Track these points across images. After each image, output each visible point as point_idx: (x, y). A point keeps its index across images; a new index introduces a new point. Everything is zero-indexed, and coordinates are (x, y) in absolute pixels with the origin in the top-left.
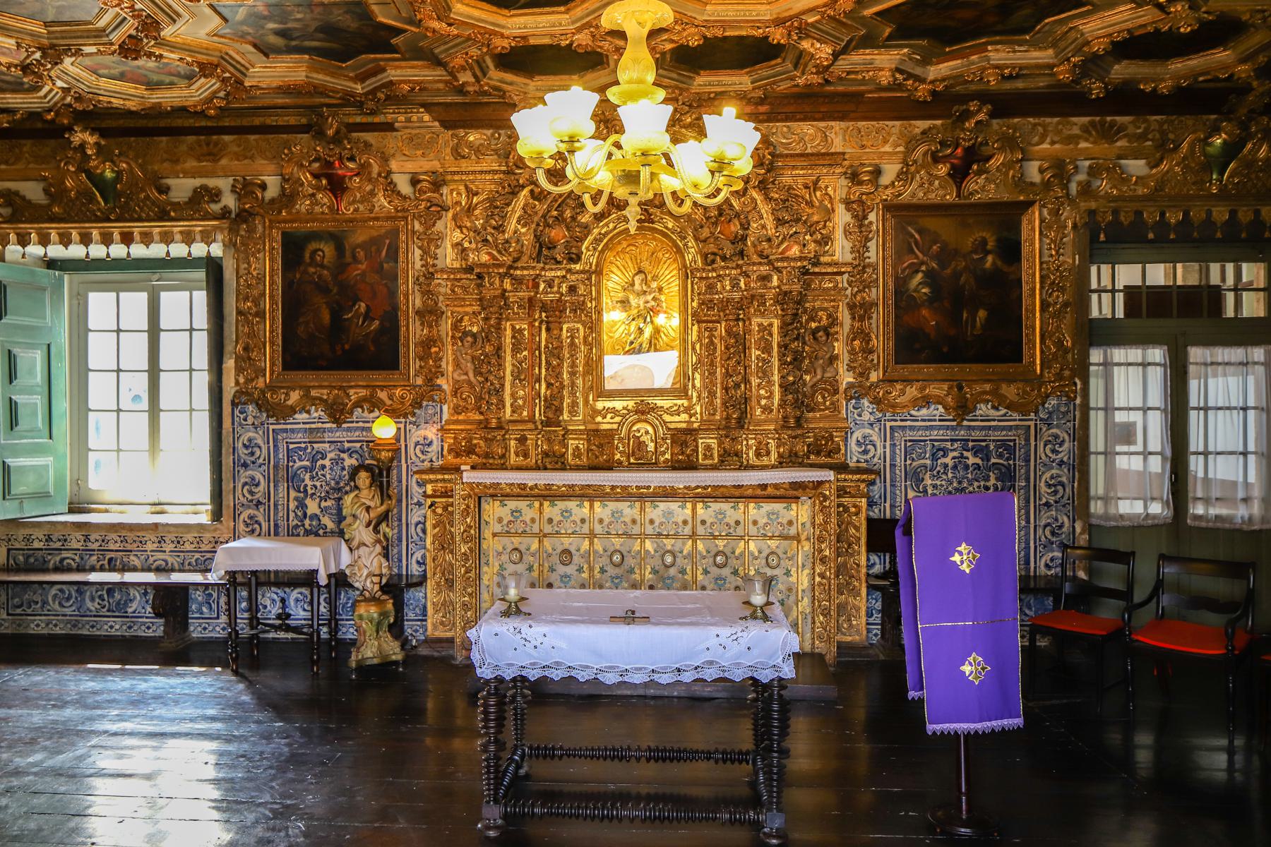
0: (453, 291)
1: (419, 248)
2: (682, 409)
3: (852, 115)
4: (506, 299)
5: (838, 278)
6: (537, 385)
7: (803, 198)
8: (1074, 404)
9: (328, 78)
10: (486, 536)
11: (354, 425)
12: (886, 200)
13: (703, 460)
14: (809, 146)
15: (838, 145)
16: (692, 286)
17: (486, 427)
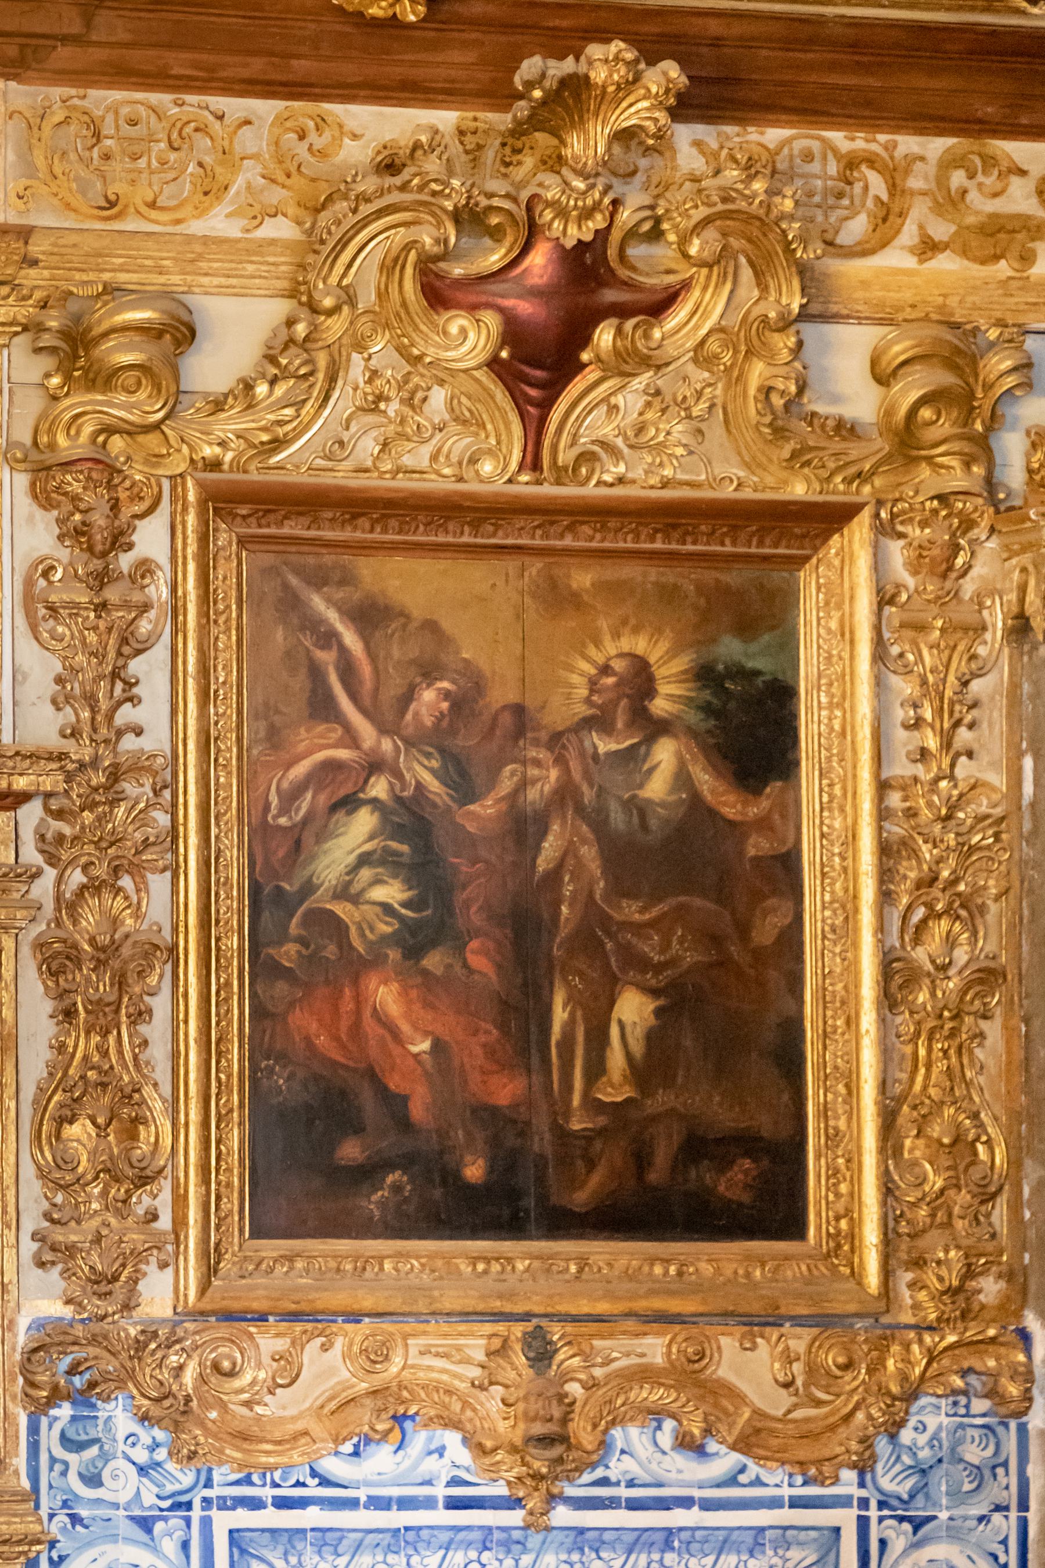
3: (63, 54)
8: (1022, 1429)
12: (215, 465)
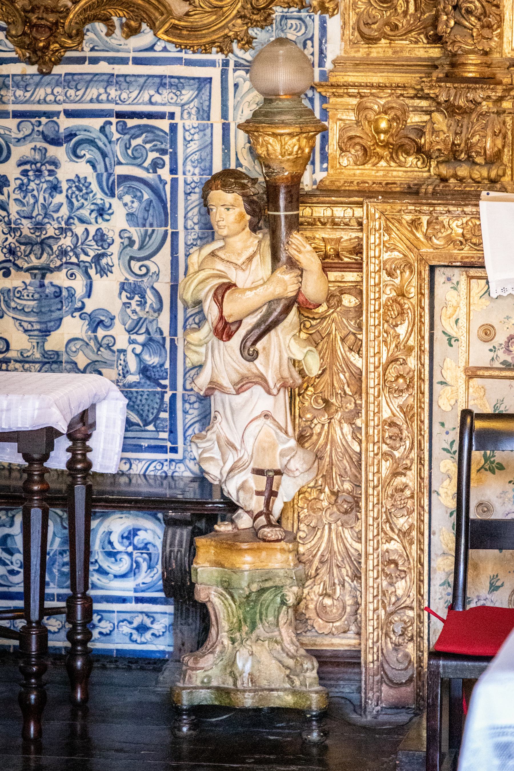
10: (448, 377)
11: (87, 68)
17: (449, 77)
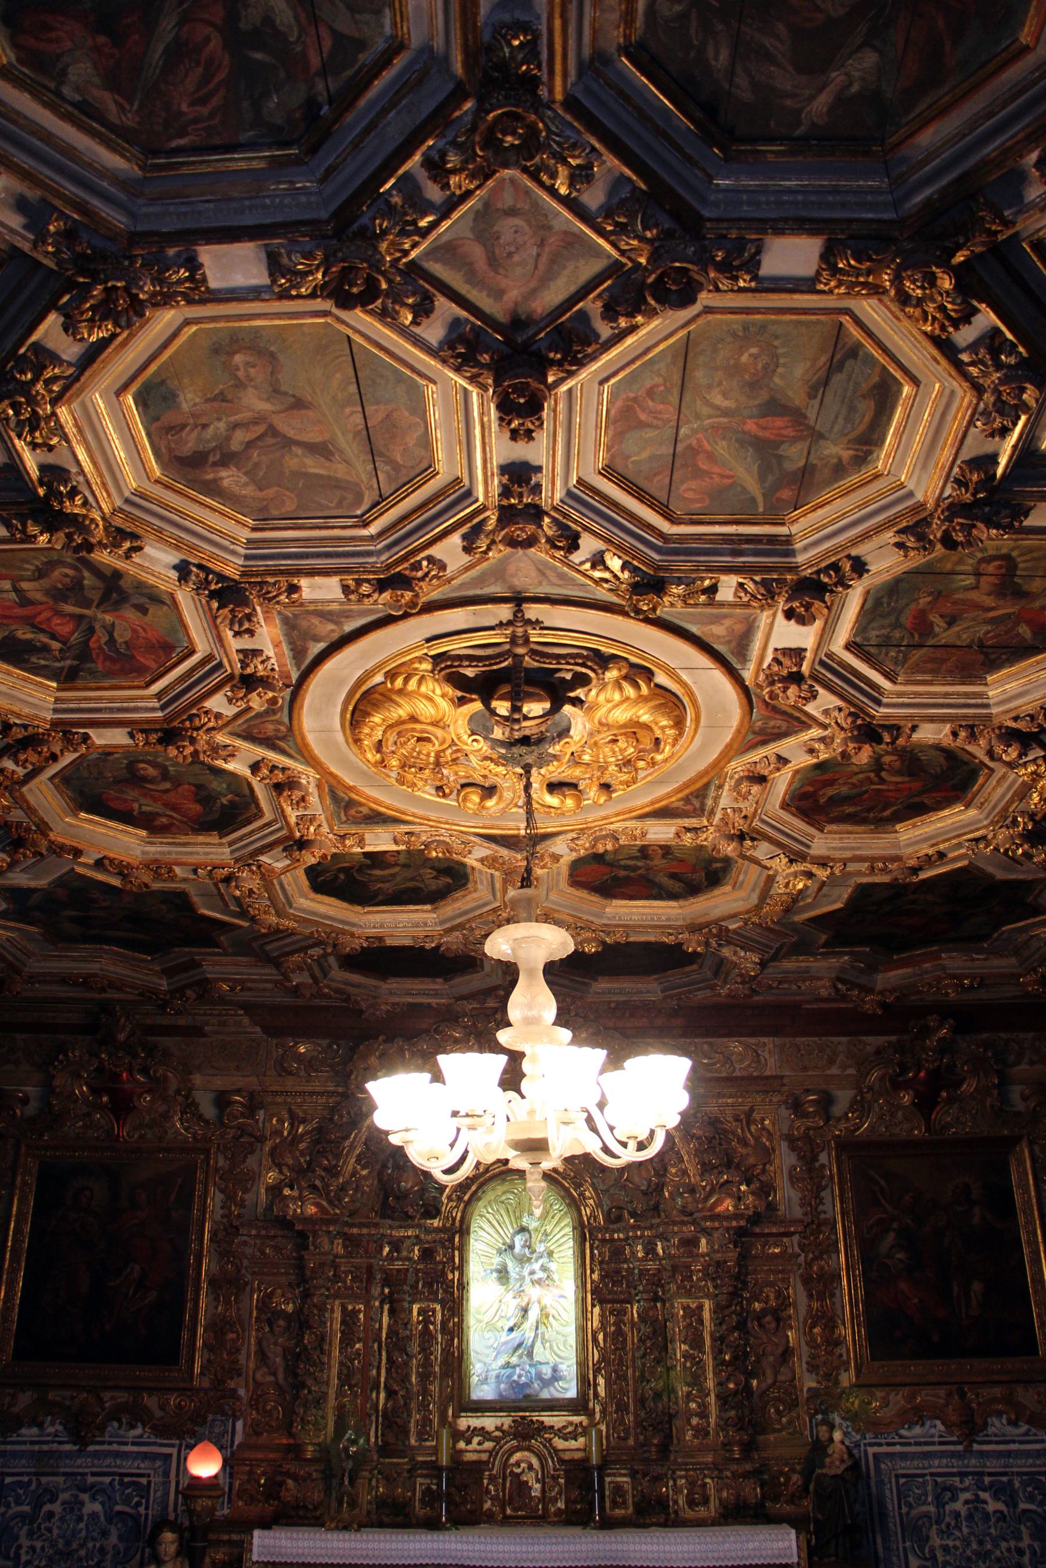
0: (263, 1253)
1: (222, 1191)
2: (580, 1430)
4: (335, 1266)
5: (785, 1240)
6: (374, 1395)
7: (734, 1133)
9: (129, 973)
11: (106, 1447)
12: (839, 1136)
13: (612, 1509)
14: (737, 1067)
15: (772, 1066)
16: (592, 1252)
